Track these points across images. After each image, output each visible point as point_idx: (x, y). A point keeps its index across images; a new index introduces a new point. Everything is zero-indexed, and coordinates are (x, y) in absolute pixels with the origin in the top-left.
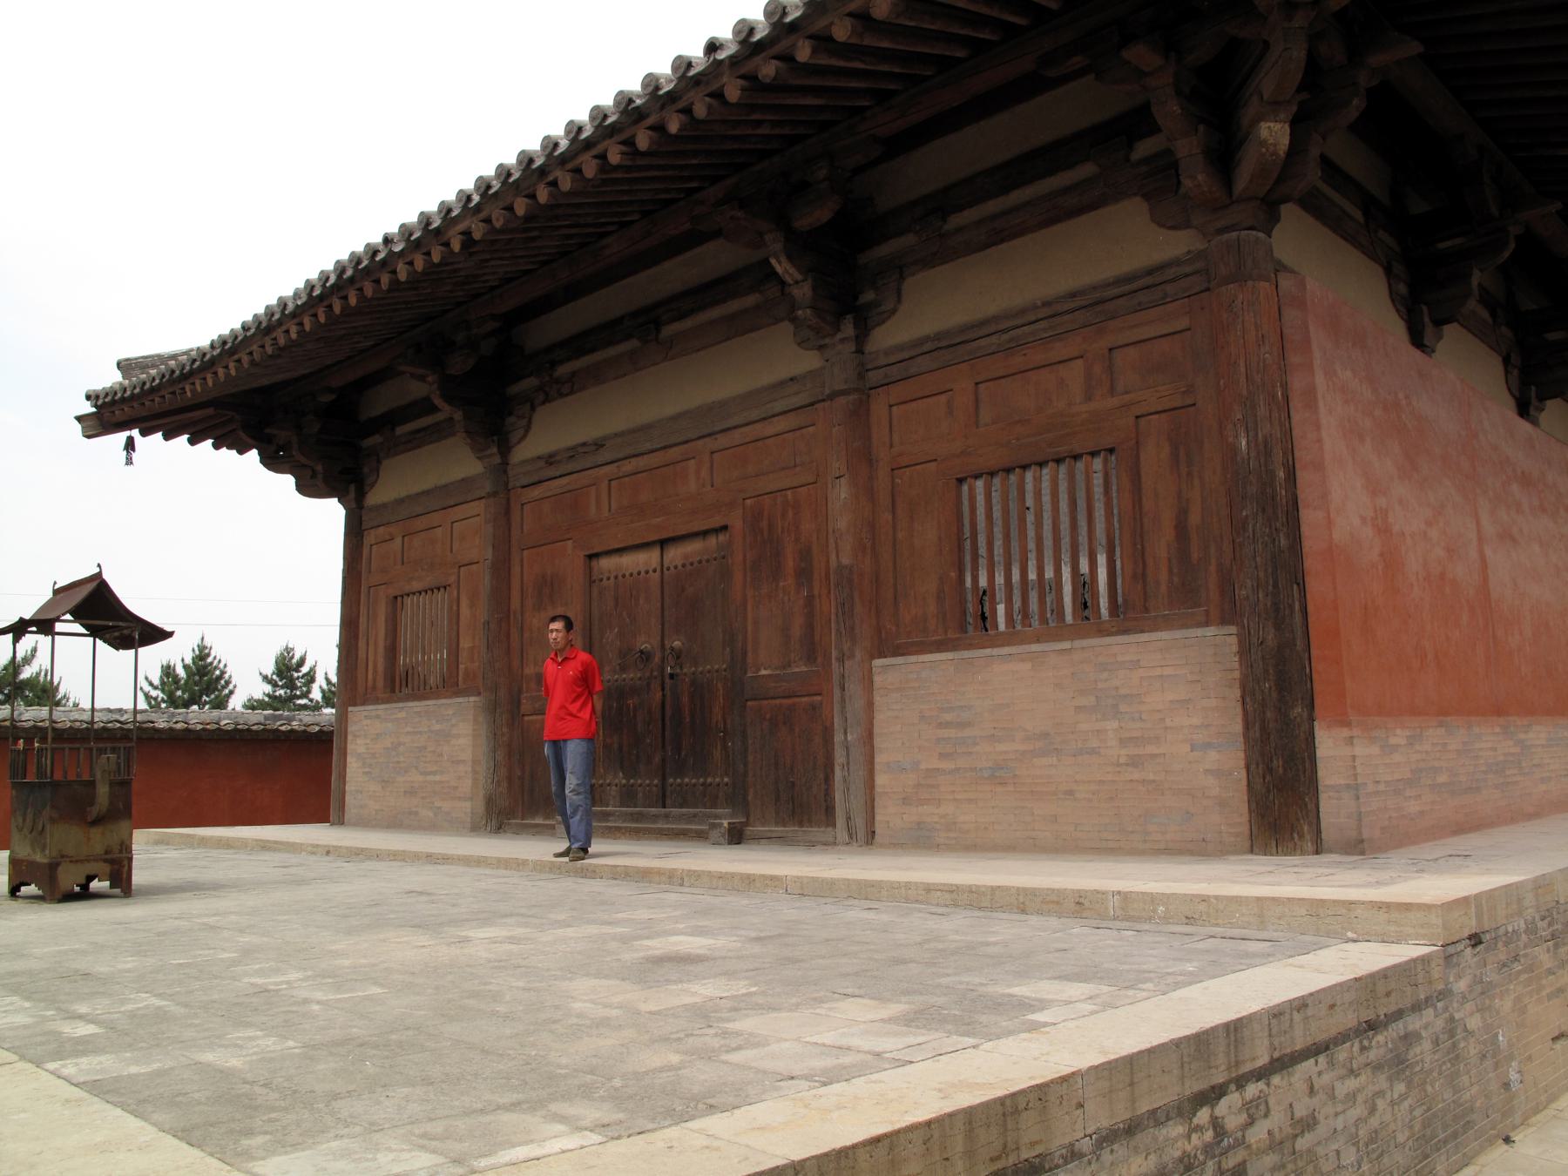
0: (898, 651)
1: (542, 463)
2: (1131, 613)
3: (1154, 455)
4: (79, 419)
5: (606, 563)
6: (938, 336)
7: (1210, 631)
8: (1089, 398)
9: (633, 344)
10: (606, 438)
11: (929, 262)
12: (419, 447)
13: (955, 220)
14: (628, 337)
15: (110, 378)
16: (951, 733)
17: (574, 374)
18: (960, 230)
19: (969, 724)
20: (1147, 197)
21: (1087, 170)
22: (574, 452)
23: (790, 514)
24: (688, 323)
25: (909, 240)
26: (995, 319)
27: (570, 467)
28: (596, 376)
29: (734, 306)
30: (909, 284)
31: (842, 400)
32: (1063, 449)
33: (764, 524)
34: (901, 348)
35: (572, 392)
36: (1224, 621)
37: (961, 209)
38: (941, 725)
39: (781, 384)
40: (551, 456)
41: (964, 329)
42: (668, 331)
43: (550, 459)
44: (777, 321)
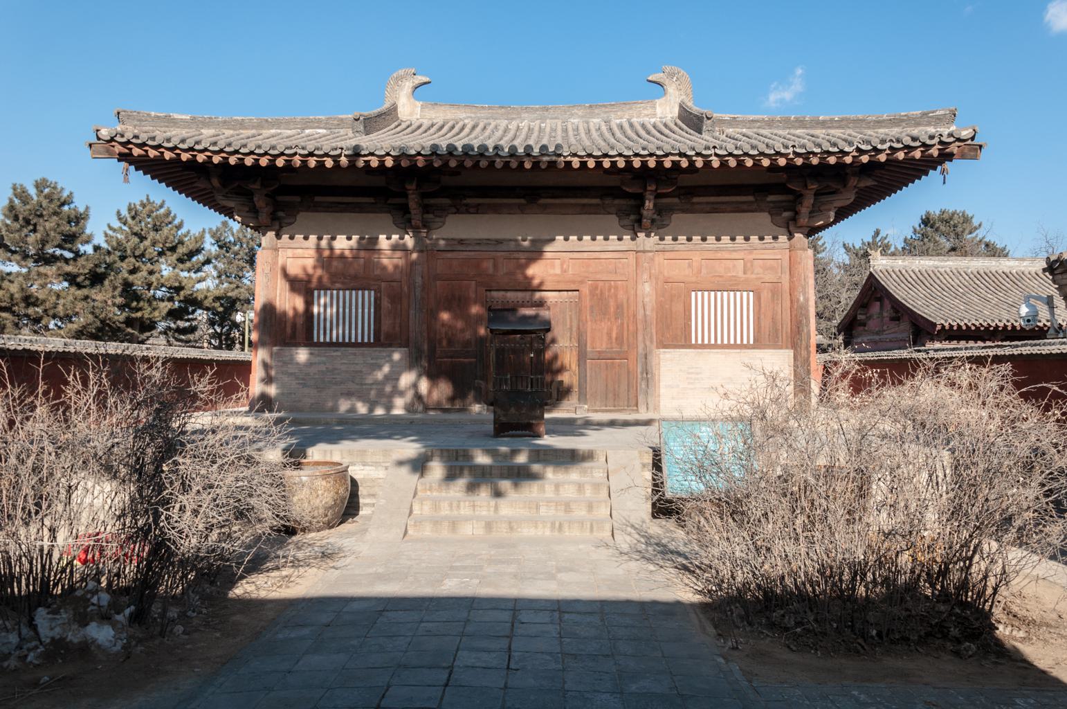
0: (665, 347)
1: (456, 242)
2: (758, 344)
3: (766, 295)
5: (495, 294)
7: (787, 351)
8: (745, 273)
9: (522, 201)
10: (504, 240)
12: (341, 212)
13: (695, 200)
14: (523, 197)
16: (693, 376)
17: (479, 205)
18: (698, 203)
19: (700, 373)
20: (771, 215)
21: (751, 198)
22: (488, 241)
23: (613, 290)
24: (557, 201)
25: (676, 200)
27: (477, 248)
28: (496, 209)
29: (585, 201)
30: (674, 216)
31: (651, 254)
32: (736, 288)
33: (598, 292)
35: (477, 213)
36: (792, 348)
37: (700, 196)
38: (689, 373)
40: (462, 240)
42: (542, 201)
43: (461, 242)
44: (609, 213)
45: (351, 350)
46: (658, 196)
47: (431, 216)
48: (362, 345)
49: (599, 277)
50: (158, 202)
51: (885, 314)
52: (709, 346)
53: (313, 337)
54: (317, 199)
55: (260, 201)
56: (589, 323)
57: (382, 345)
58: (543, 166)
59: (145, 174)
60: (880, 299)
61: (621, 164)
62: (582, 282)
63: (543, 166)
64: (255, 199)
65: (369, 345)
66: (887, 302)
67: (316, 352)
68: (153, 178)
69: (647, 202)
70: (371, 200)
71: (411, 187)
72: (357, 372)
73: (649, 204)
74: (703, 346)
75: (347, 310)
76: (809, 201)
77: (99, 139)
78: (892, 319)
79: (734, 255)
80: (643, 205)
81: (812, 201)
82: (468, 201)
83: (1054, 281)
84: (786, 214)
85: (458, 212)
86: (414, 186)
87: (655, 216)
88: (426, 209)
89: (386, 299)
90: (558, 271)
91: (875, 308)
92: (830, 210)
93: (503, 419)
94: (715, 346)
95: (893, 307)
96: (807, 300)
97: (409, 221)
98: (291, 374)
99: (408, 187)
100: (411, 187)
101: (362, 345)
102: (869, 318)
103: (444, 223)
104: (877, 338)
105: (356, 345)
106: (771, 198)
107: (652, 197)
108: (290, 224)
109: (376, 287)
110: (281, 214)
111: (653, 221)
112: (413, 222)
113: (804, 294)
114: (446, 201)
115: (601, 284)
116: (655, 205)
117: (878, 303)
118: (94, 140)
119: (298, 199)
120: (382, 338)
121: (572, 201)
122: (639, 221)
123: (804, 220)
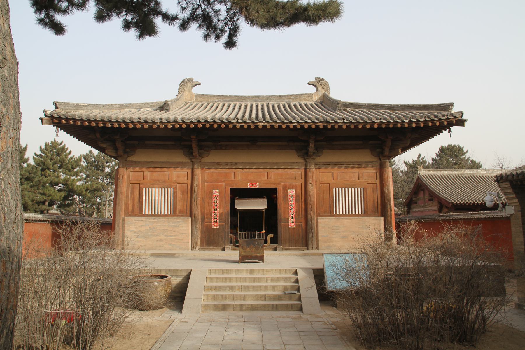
2: (366, 213)
4: (41, 119)
6: (331, 162)
9: (248, 143)
11: (329, 148)
13: (334, 143)
15: (51, 108)
16: (335, 231)
26: (343, 162)
28: (235, 148)
29: (280, 143)
30: (324, 151)
34: (323, 162)
39: (294, 163)
41: (336, 162)
42: (259, 143)
44: (292, 150)
45: (162, 218)
46: (316, 141)
47: (203, 151)
48: (167, 216)
49: (288, 181)
50: (60, 142)
51: (426, 198)
52: (343, 215)
53: (142, 212)
54: (146, 142)
55: (119, 144)
56: (282, 204)
57: (177, 216)
58: (260, 127)
59: (64, 132)
60: (423, 190)
61: (299, 126)
62: (279, 184)
63: (260, 127)
64: (117, 143)
65: (170, 216)
66: (426, 191)
67: (144, 220)
68: (68, 134)
69: (311, 144)
70: (173, 143)
71: (193, 137)
72: (164, 230)
73: (312, 145)
74: (339, 216)
75: (160, 198)
76: (389, 143)
77: (45, 116)
78: (430, 200)
79: (354, 170)
80: (308, 146)
81: (390, 144)
82: (221, 143)
83: (499, 186)
84: (378, 150)
85: (216, 149)
86: (195, 137)
87: (315, 151)
88: (200, 147)
89: (180, 193)
90: (266, 178)
91: (421, 195)
92: (399, 148)
93: (244, 254)
94: (346, 215)
95: (429, 194)
96: (389, 192)
97: (192, 153)
98: (132, 231)
99: (192, 137)
100: (193, 137)
101: (167, 216)
102: (419, 199)
103: (209, 154)
104: (422, 209)
105: (164, 216)
106: (371, 142)
107: (313, 142)
108: (132, 155)
109: (174, 187)
110: (128, 150)
111: (314, 153)
112: (194, 154)
113: (388, 190)
114: (211, 143)
115: (288, 185)
116: (315, 146)
117: (422, 192)
118: (43, 116)
119: (136, 143)
120: (177, 212)
121: (273, 143)
122: (307, 154)
123: (387, 152)
